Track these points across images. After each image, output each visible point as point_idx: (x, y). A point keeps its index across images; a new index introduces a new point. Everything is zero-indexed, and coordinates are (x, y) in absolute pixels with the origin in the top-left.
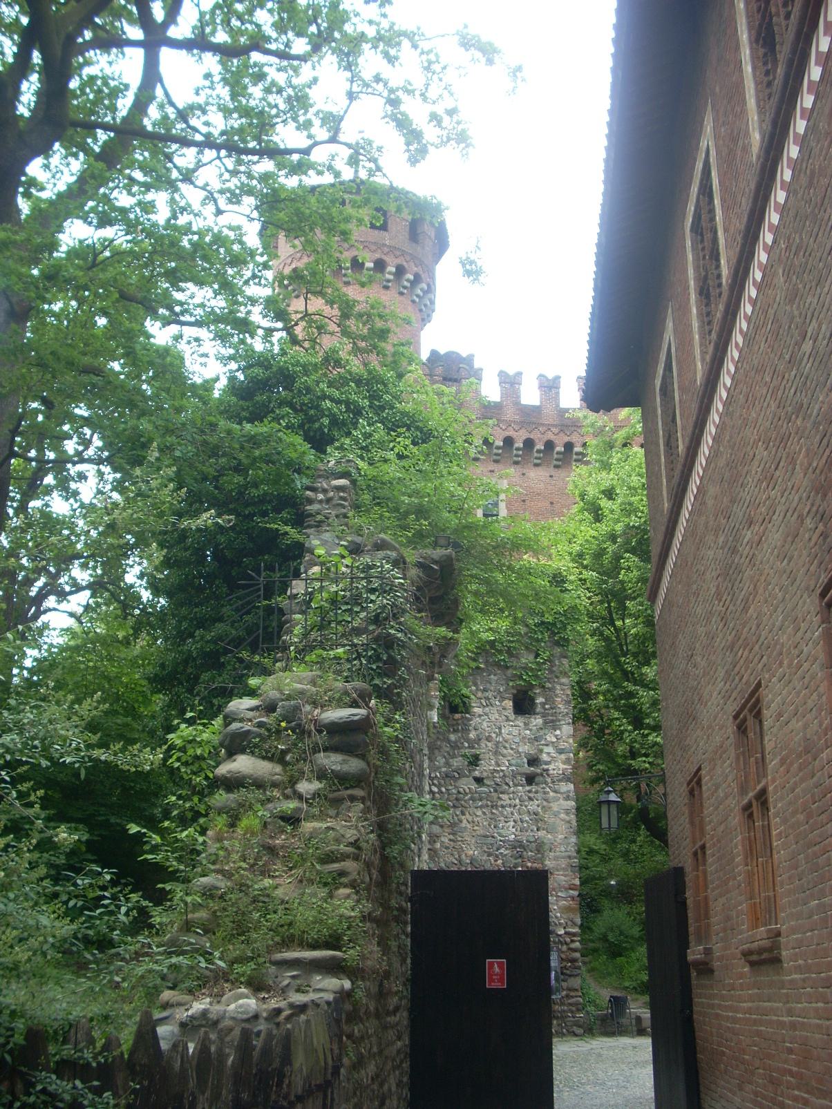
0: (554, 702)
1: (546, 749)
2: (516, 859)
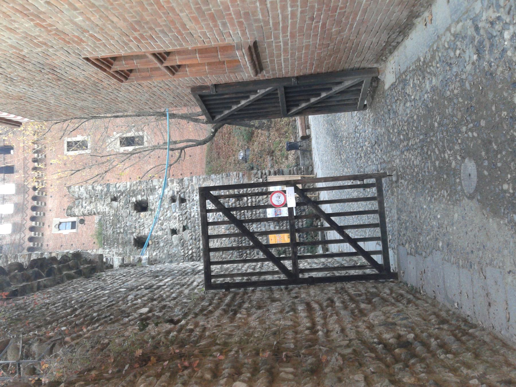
0: (140, 190)
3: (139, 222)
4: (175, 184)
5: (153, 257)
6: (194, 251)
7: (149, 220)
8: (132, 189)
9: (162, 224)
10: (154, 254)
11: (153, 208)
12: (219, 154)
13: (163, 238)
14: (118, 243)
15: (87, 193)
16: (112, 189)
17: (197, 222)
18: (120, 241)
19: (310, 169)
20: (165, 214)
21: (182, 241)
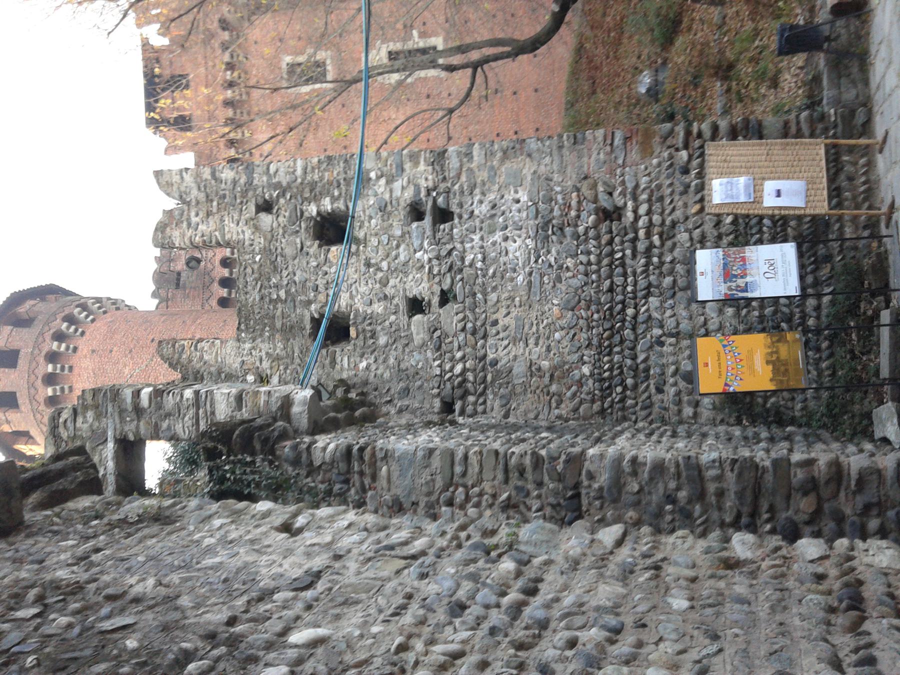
0: (330, 183)
1: (397, 193)
2: (565, 236)
3: (326, 273)
4: (422, 167)
5: (361, 374)
6: (468, 365)
7: (351, 270)
8: (309, 178)
9: (384, 283)
10: (363, 365)
11: (361, 235)
12: (594, 83)
13: (387, 323)
14: (273, 328)
15: (199, 189)
16: (259, 179)
17: (479, 281)
18: (278, 324)
19: (860, 118)
20: (394, 253)
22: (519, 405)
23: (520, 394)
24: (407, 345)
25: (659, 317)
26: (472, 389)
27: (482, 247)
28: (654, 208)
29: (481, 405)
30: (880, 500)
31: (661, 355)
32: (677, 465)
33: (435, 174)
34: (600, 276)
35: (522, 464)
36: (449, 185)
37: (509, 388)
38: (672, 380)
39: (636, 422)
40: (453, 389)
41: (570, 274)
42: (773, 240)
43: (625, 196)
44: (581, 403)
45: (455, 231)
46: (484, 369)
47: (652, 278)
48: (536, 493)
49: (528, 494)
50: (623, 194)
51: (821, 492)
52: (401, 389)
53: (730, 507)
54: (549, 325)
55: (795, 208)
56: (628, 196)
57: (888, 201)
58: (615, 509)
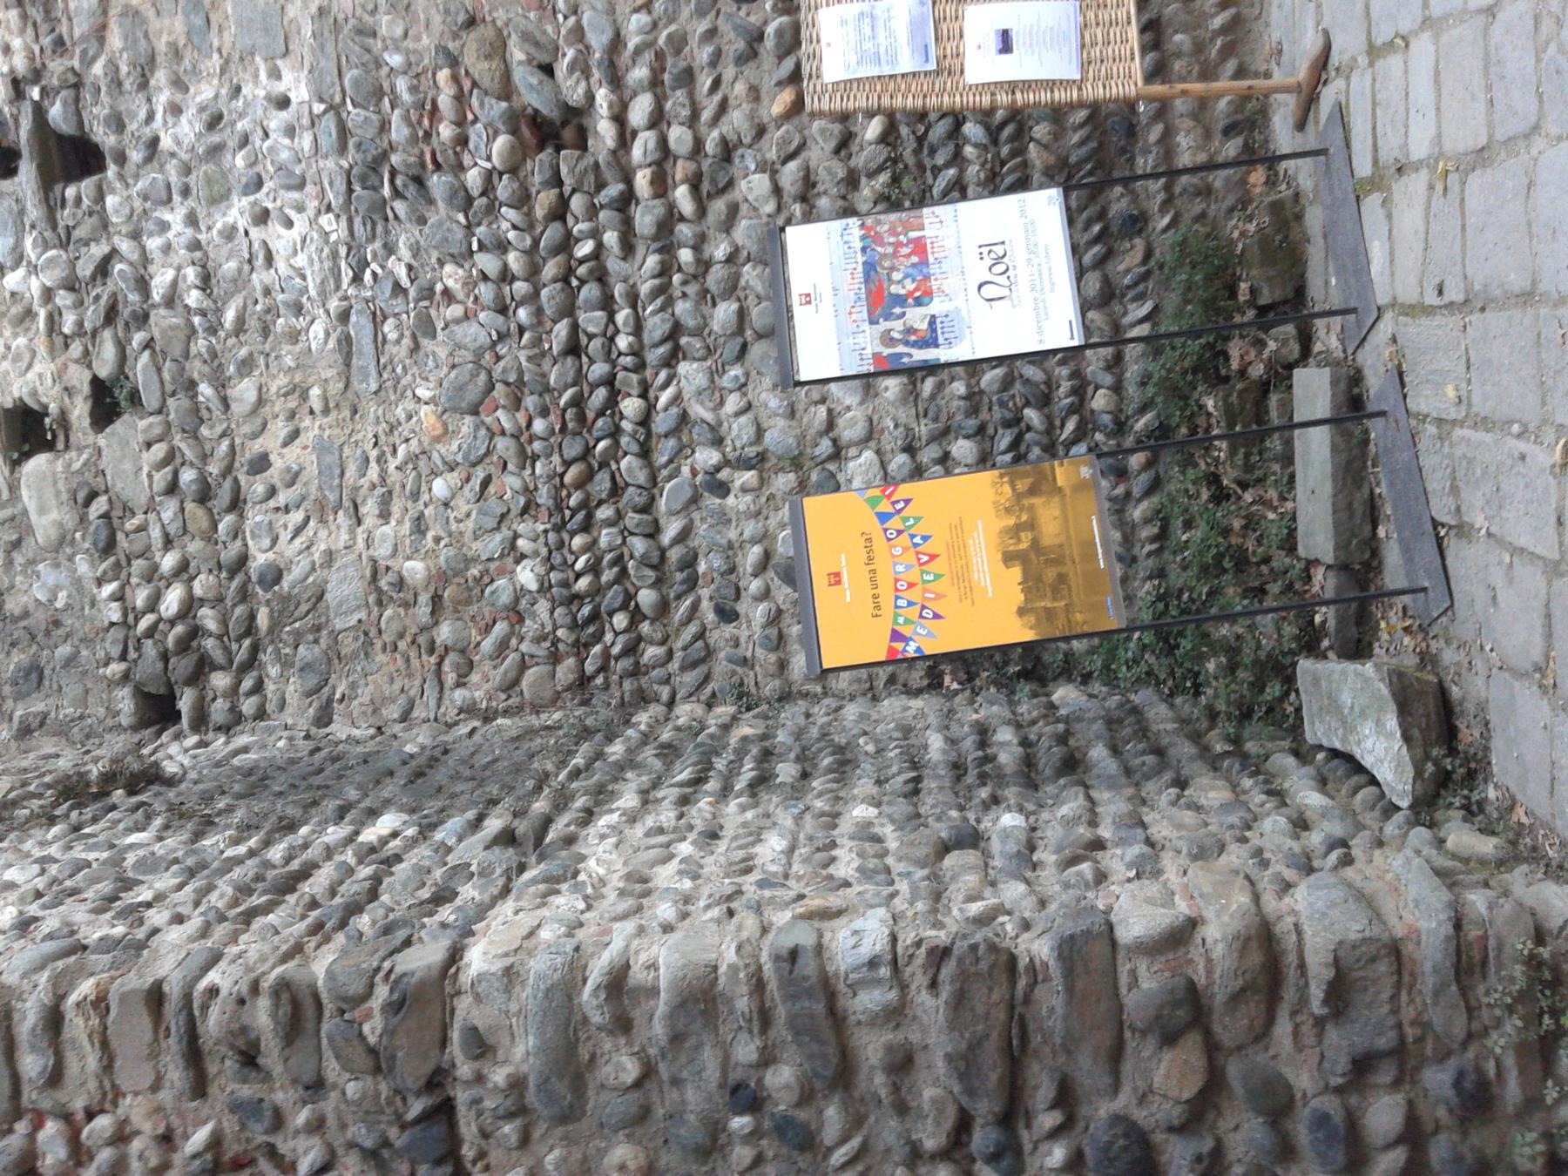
2: (431, 201)
17: (200, 345)
21: (100, 505)
22: (353, 686)
23: (354, 656)
24: (17, 544)
25: (709, 417)
26: (218, 655)
27: (195, 246)
28: (668, 105)
29: (249, 694)
30: (1402, 1037)
31: (724, 519)
32: (759, 986)
33: (30, 31)
34: (539, 312)
35: (244, 1030)
36: (76, 63)
37: (323, 642)
38: (755, 585)
39: (671, 703)
40: (165, 657)
41: (455, 311)
42: (994, 185)
43: (587, 74)
44: (523, 666)
45: (111, 201)
46: (244, 595)
47: (681, 307)
48: (302, 1117)
49: (278, 1121)
50: (581, 67)
51: (1217, 1028)
52: (18, 669)
53: (933, 1101)
54: (413, 458)
55: (1051, 84)
56: (596, 74)
57: (1310, 44)
58: (569, 1141)
